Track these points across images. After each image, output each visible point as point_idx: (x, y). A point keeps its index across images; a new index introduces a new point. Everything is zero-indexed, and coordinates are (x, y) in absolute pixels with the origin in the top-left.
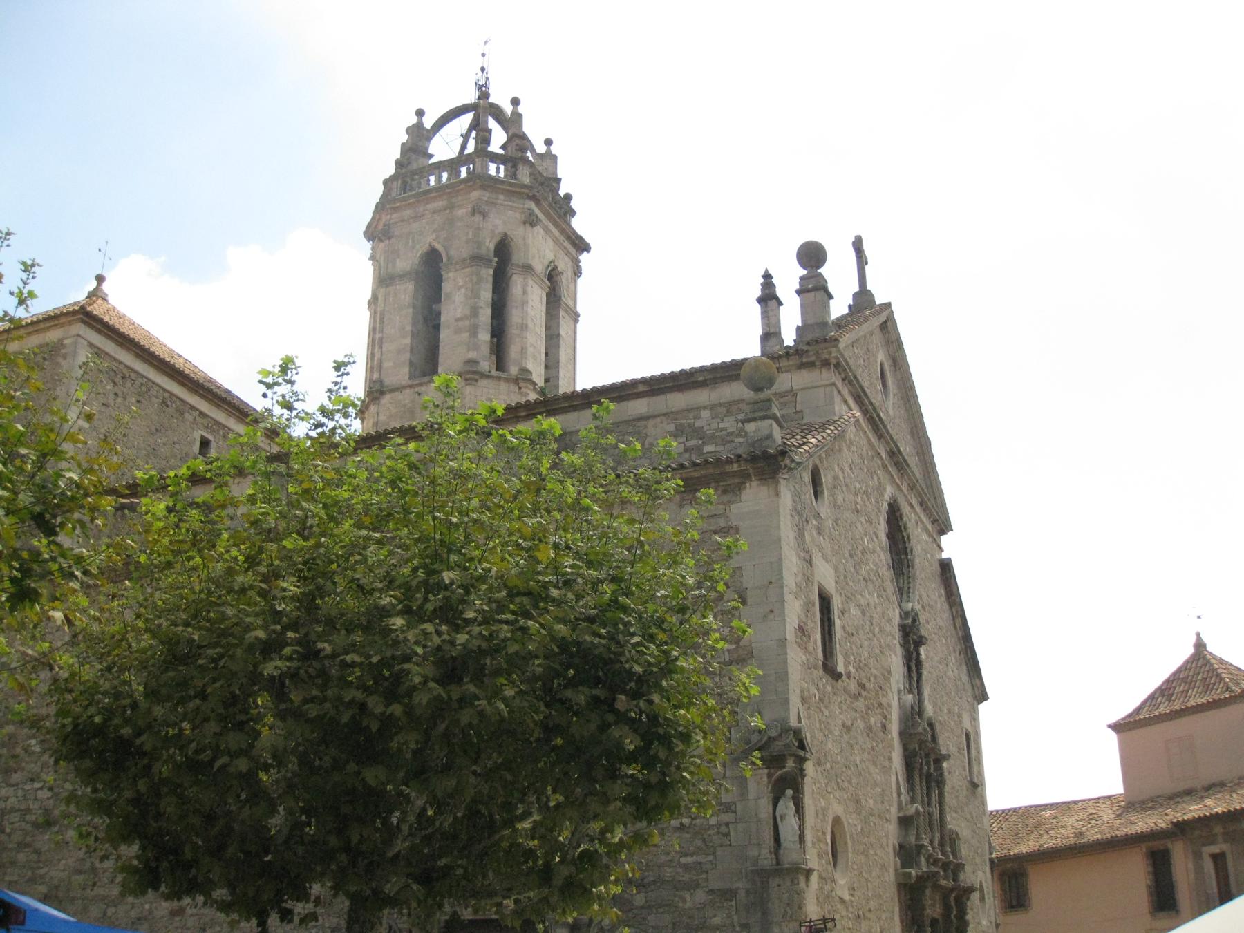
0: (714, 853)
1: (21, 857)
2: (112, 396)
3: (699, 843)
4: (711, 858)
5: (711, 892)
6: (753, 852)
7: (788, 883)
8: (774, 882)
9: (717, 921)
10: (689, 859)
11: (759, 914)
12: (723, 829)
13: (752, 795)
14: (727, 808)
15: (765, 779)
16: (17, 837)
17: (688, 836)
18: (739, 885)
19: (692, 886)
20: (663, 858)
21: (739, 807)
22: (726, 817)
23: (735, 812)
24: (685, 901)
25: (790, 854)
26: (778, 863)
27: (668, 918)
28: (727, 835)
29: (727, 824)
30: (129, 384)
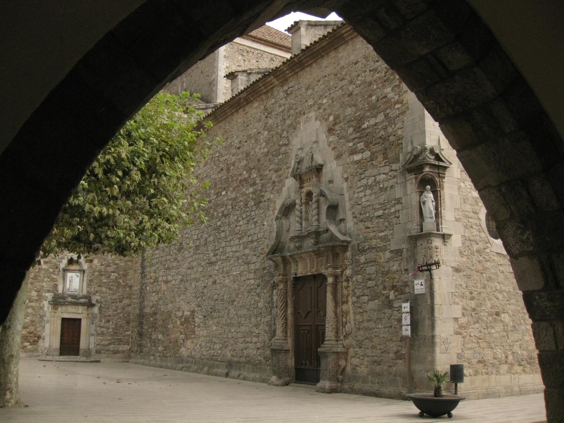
0: (393, 229)
1: (175, 264)
2: (242, 61)
3: (386, 224)
4: (391, 232)
5: (391, 252)
6: (409, 226)
7: (426, 243)
8: (419, 243)
9: (395, 268)
10: (383, 234)
11: (412, 263)
12: (397, 215)
13: (409, 192)
14: (399, 201)
15: (414, 181)
16: (174, 256)
17: (382, 220)
18: (404, 246)
19: (384, 249)
20: (372, 234)
21: (403, 200)
22: (398, 207)
23: (401, 203)
24: (381, 259)
25: (429, 224)
26: (422, 230)
27: (374, 268)
28: (398, 217)
29: (399, 211)
30: (251, 54)
